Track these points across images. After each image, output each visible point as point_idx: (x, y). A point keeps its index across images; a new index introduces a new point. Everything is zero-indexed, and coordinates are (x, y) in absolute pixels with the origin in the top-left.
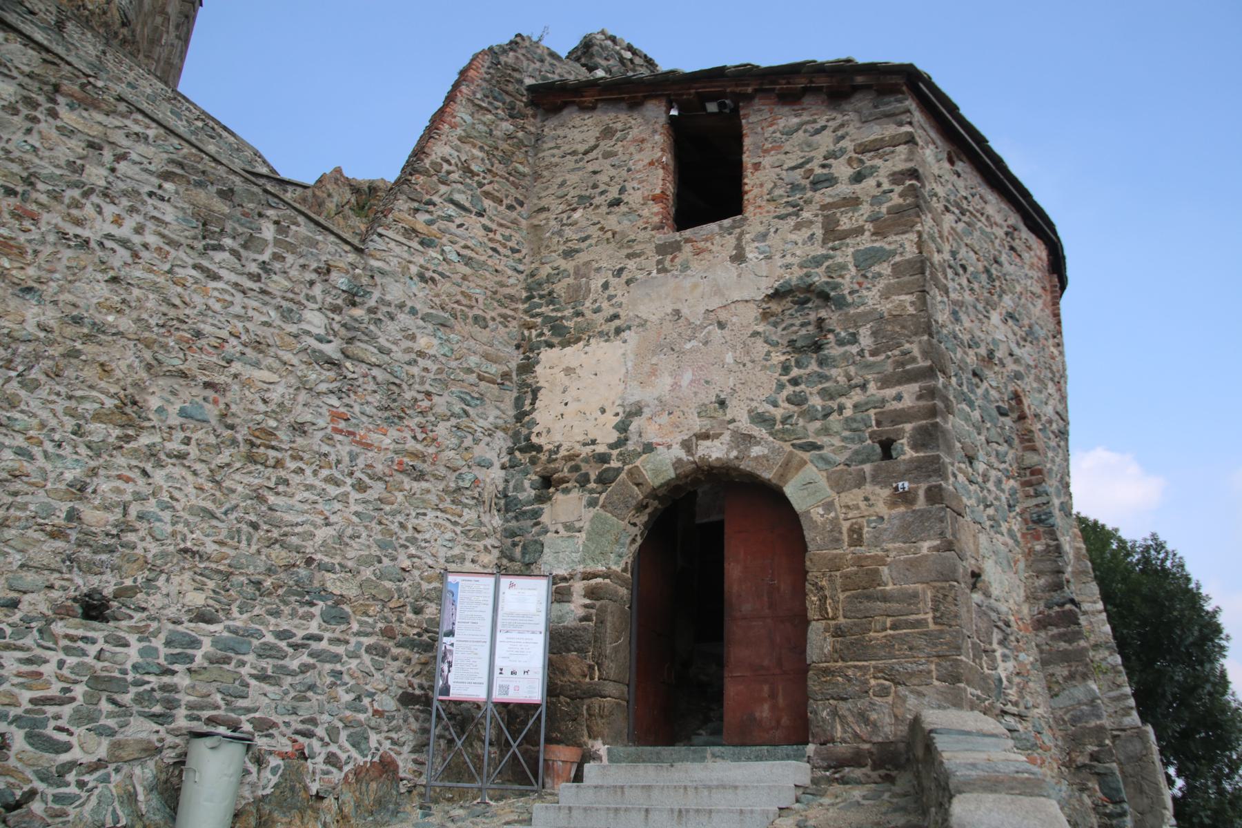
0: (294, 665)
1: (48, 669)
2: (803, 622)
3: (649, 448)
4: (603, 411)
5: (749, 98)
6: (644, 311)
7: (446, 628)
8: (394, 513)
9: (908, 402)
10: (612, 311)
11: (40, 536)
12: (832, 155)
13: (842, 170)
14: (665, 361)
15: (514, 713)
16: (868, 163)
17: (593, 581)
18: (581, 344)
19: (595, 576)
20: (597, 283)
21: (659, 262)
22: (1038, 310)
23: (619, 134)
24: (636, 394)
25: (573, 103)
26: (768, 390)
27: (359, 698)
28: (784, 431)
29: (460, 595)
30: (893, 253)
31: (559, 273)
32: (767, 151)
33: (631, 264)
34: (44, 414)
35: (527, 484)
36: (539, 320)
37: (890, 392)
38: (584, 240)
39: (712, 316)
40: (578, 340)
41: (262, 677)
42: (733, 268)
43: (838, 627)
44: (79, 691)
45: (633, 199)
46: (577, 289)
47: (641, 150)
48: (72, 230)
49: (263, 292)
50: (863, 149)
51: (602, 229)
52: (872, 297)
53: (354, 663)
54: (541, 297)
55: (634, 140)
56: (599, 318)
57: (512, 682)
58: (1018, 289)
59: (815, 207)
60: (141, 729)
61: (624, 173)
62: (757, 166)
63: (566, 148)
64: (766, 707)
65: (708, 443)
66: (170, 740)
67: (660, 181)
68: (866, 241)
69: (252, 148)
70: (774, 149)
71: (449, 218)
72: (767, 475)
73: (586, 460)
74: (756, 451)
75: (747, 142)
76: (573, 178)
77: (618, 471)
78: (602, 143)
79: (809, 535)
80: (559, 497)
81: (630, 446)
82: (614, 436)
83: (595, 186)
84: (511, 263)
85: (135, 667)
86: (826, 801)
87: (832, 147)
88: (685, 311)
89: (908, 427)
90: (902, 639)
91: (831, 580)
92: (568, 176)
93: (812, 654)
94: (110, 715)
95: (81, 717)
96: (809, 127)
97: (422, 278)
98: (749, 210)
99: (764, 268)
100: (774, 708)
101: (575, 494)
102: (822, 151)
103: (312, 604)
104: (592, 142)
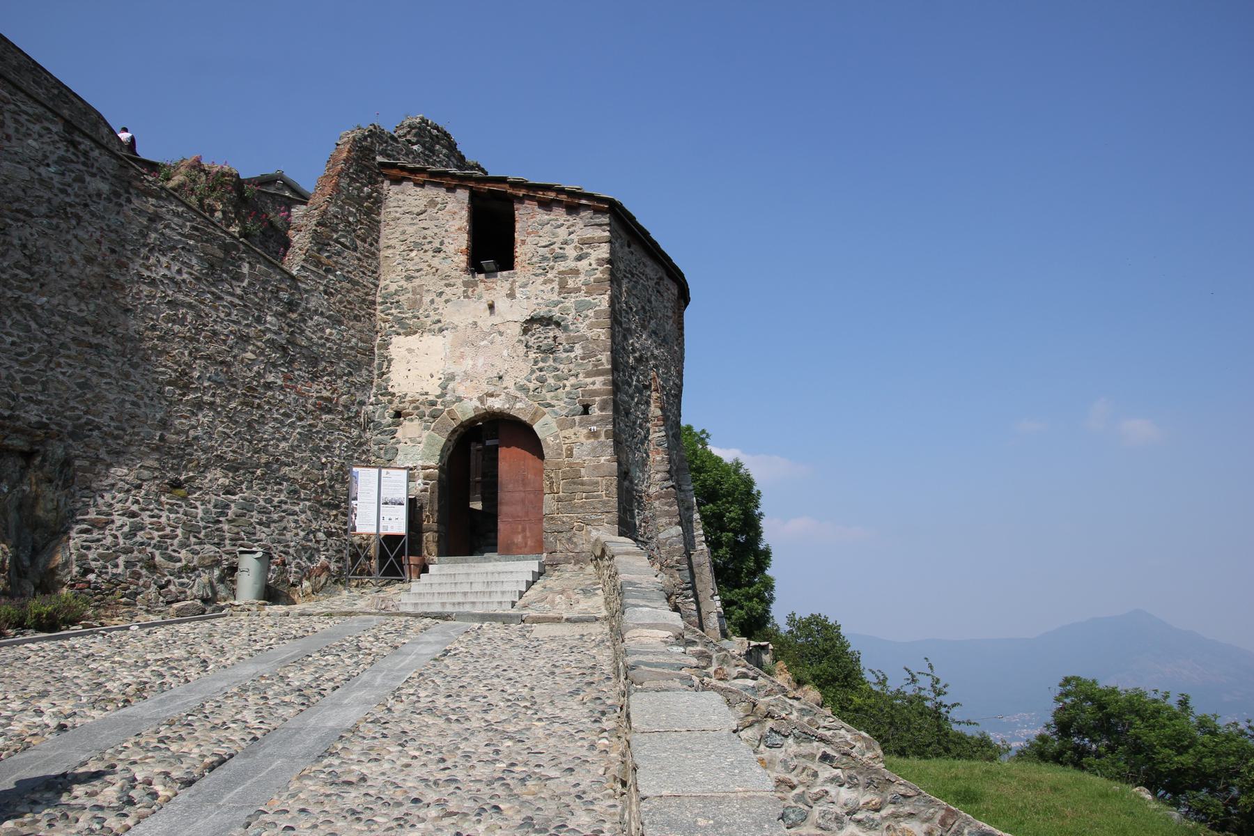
0: (275, 516)
1: (163, 520)
2: (541, 492)
3: (459, 399)
5: (521, 200)
6: (456, 320)
8: (318, 432)
9: (598, 386)
10: (437, 318)
11: (147, 450)
12: (566, 243)
13: (571, 252)
14: (468, 350)
15: (391, 540)
19: (429, 468)
20: (427, 299)
22: (669, 326)
24: (453, 368)
25: (409, 180)
31: (403, 290)
33: (448, 290)
34: (143, 382)
36: (390, 318)
37: (589, 380)
38: (418, 271)
40: (416, 332)
41: (261, 523)
44: (179, 531)
45: (450, 249)
46: (415, 302)
48: (146, 273)
49: (245, 306)
52: (583, 327)
53: (303, 516)
57: (390, 524)
59: (555, 272)
60: (209, 550)
62: (523, 242)
63: (405, 208)
66: (225, 556)
67: (463, 241)
68: (582, 296)
69: (96, 112)
70: (534, 230)
71: (339, 254)
74: (518, 405)
75: (518, 226)
76: (410, 230)
77: (442, 411)
79: (545, 451)
80: (406, 423)
81: (448, 398)
82: (439, 392)
83: (425, 238)
89: (597, 399)
93: (546, 511)
94: (196, 544)
95: (183, 545)
97: (325, 292)
98: (518, 268)
99: (525, 303)
100: (525, 537)
101: (417, 422)
102: (561, 239)
103: (281, 484)
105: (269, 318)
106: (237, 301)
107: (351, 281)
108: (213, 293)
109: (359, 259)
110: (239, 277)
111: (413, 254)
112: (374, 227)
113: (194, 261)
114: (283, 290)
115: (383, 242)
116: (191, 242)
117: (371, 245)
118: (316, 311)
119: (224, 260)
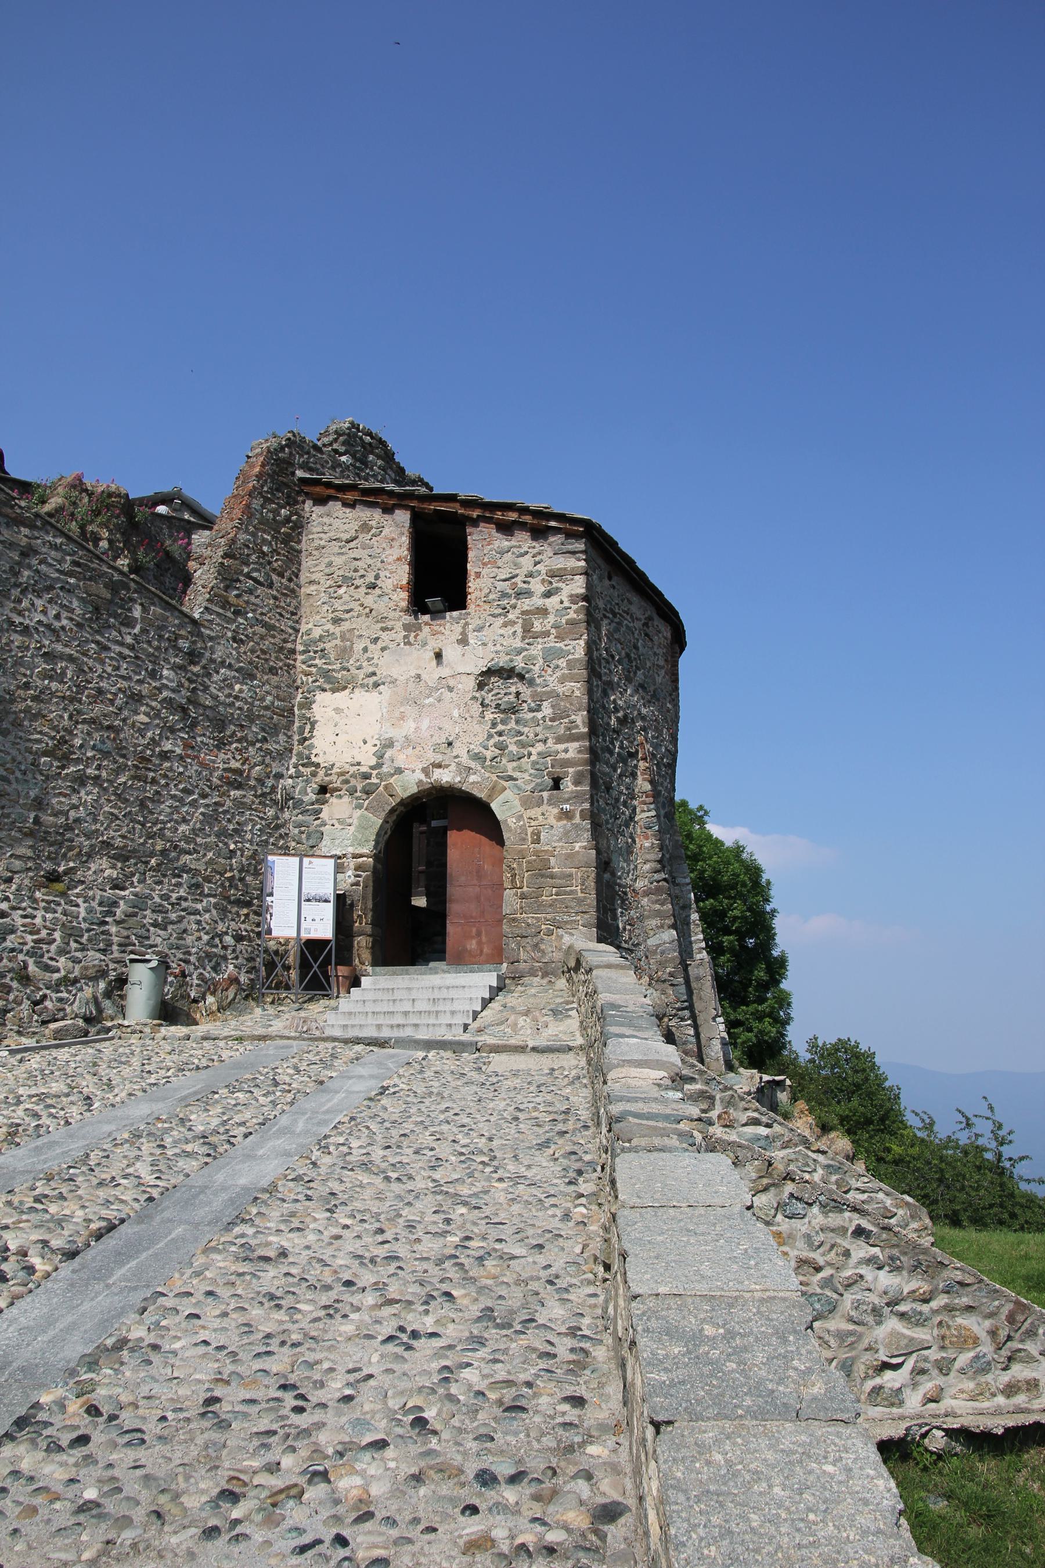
0: (173, 916)
1: (38, 921)
2: (500, 887)
3: (399, 771)
4: (365, 742)
5: (475, 522)
6: (395, 672)
7: (269, 891)
8: (225, 812)
9: (571, 755)
10: (371, 669)
11: (18, 835)
12: (530, 575)
13: (537, 586)
14: (409, 710)
15: (314, 946)
16: (555, 585)
17: (361, 860)
18: (347, 691)
19: (361, 856)
20: (358, 646)
21: (405, 637)
23: (374, 531)
24: (391, 733)
25: (336, 499)
26: (482, 737)
27: (213, 938)
28: (492, 767)
29: (277, 869)
30: (569, 653)
31: (330, 634)
32: (485, 564)
33: (384, 635)
34: (14, 752)
35: (309, 790)
36: (314, 670)
37: (561, 747)
38: (348, 611)
39: (444, 682)
40: (345, 688)
41: (155, 925)
42: (459, 648)
43: (523, 893)
44: (57, 935)
46: (344, 650)
47: (391, 547)
48: (17, 620)
49: (137, 658)
50: (553, 574)
51: (362, 605)
52: (552, 681)
53: (207, 916)
54: (316, 652)
55: (386, 538)
56: (361, 674)
57: (313, 926)
58: (648, 664)
59: (517, 611)
60: (93, 957)
61: (379, 565)
62: (478, 575)
63: (332, 534)
64: (474, 942)
65: (440, 770)
66: (112, 966)
67: (403, 574)
68: (551, 642)
71: (251, 592)
72: (482, 795)
73: (353, 776)
74: (472, 778)
75: (471, 555)
76: (338, 561)
77: (377, 786)
78: (361, 536)
79: (506, 835)
80: (333, 800)
81: (385, 769)
82: (373, 761)
83: (356, 570)
84: (290, 623)
85: (84, 920)
86: (516, 995)
87: (531, 568)
88: (423, 677)
89: (571, 770)
90: (562, 901)
91: (520, 865)
92: (333, 558)
93: (506, 910)
95: (62, 952)
96: (515, 550)
97: (234, 639)
98: (471, 607)
100: (480, 943)
101: (346, 799)
103: (180, 876)
104: (353, 533)
105: (165, 672)
106: (127, 652)
107: (265, 625)
108: (97, 643)
109: (275, 598)
110: (129, 623)
111: (342, 591)
112: (294, 558)
113: (75, 604)
114: (182, 637)
115: (304, 577)
116: (72, 581)
117: (290, 580)
118: (223, 662)
119: (111, 602)
